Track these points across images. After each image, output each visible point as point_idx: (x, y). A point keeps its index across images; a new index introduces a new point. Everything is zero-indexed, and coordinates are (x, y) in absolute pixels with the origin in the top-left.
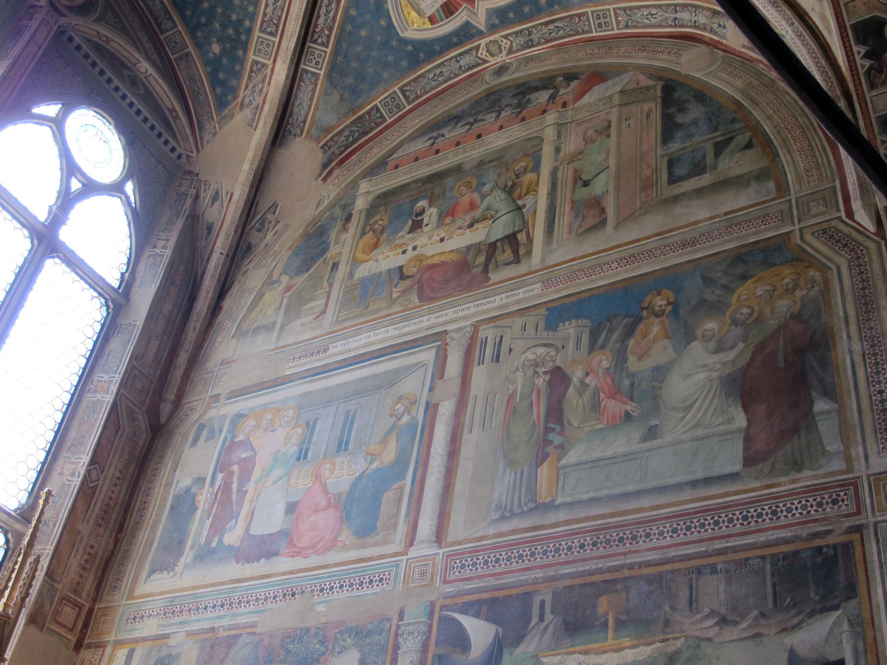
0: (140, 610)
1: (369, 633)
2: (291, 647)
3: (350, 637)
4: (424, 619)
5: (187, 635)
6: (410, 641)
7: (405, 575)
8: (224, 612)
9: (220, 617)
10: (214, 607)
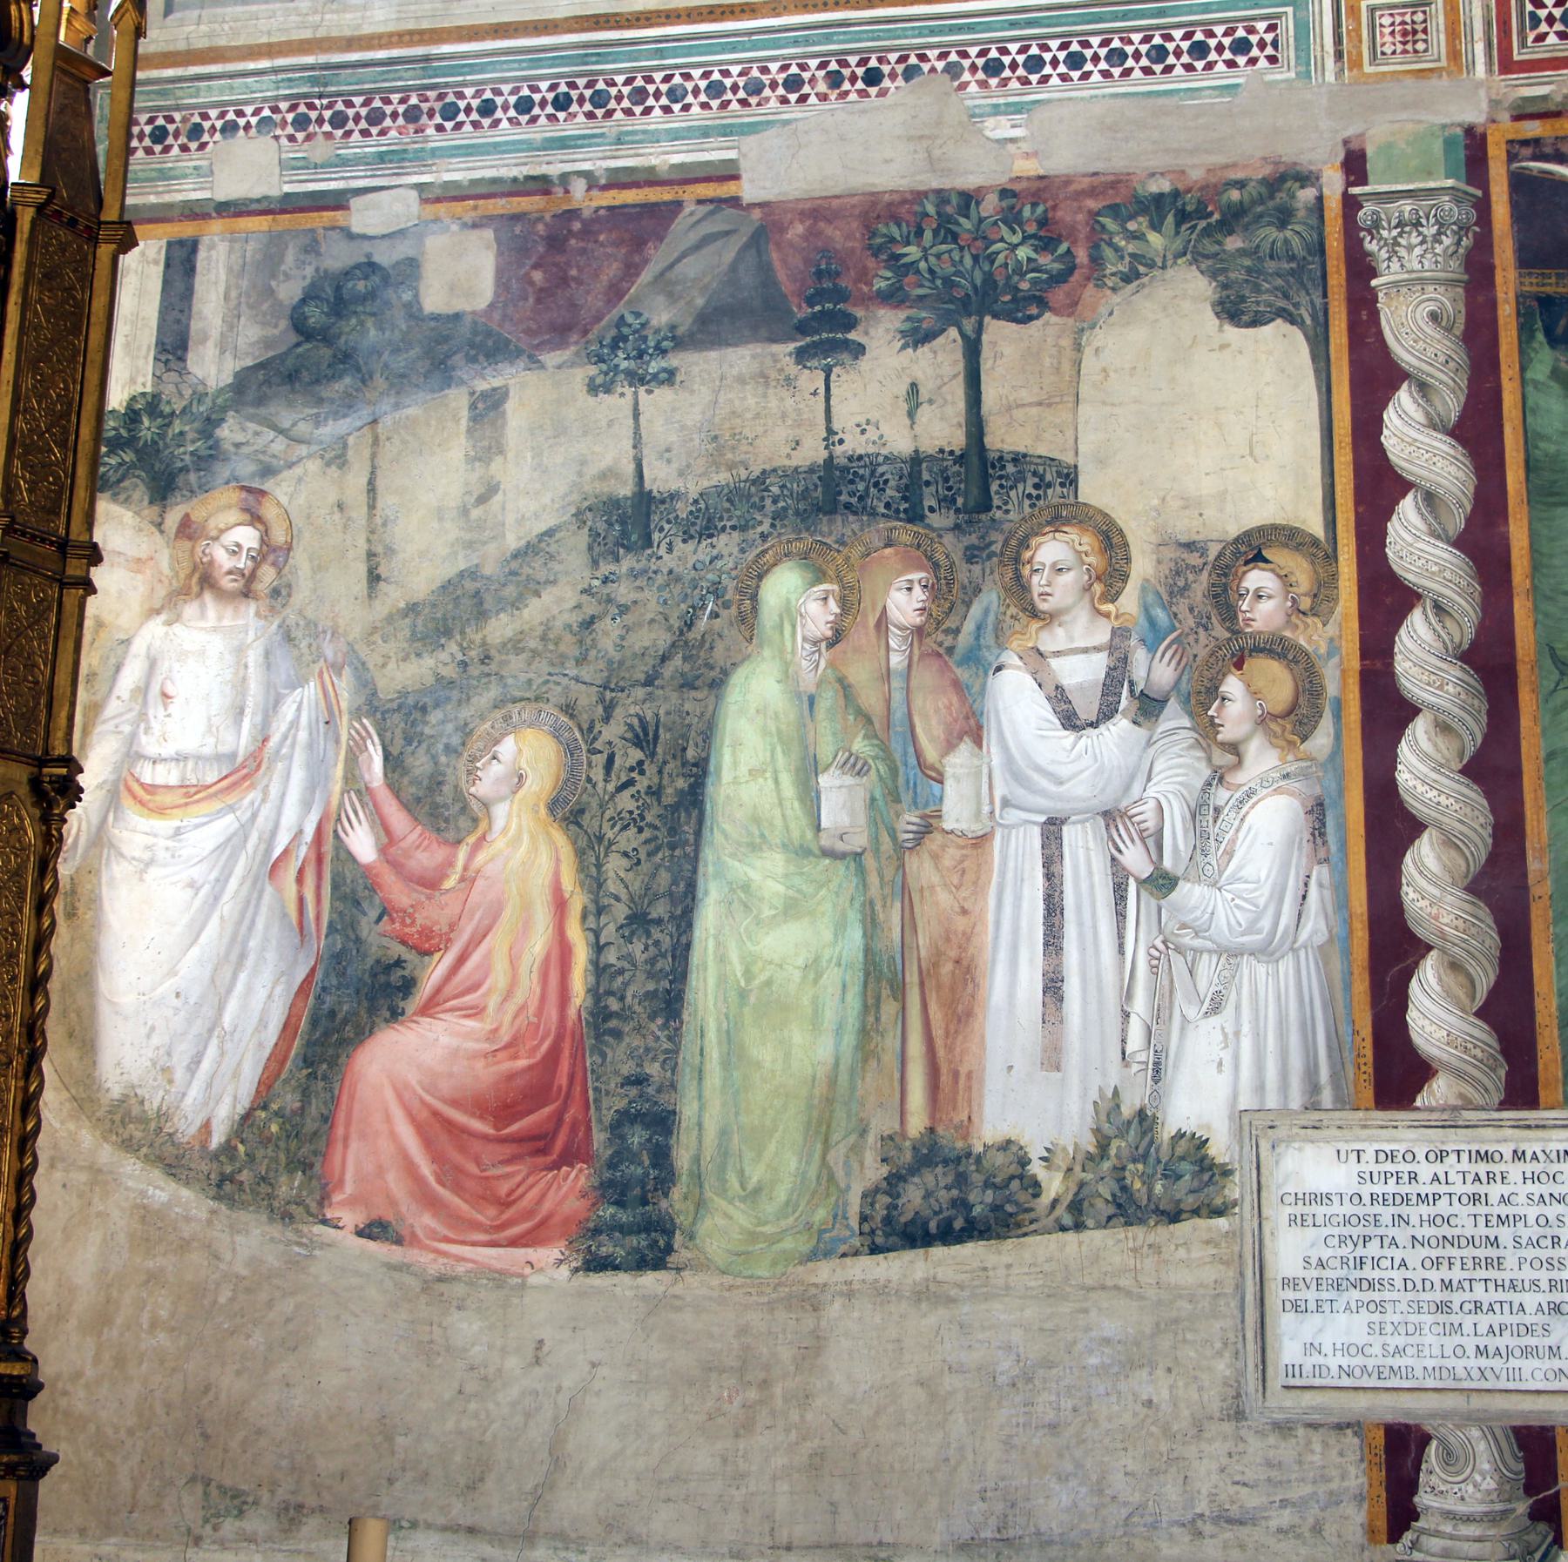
0: (178, 108)
1: (1234, 218)
2: (913, 251)
3: (1156, 227)
4: (1450, 183)
5: (424, 201)
6: (1410, 248)
7: (1338, 40)
8: (575, 124)
9: (563, 143)
10: (524, 106)
